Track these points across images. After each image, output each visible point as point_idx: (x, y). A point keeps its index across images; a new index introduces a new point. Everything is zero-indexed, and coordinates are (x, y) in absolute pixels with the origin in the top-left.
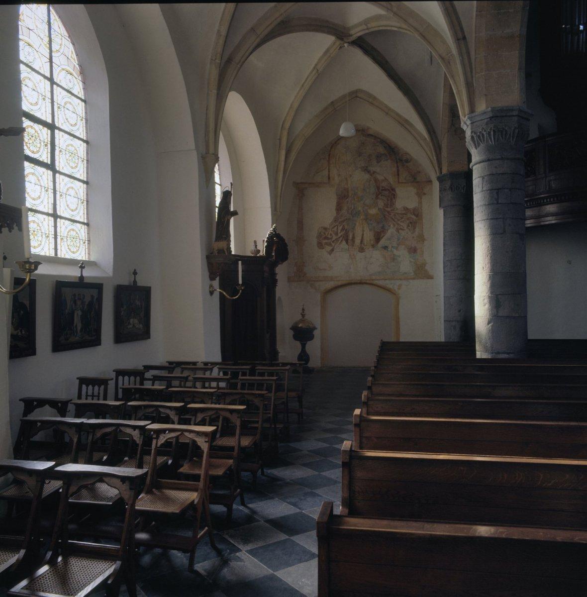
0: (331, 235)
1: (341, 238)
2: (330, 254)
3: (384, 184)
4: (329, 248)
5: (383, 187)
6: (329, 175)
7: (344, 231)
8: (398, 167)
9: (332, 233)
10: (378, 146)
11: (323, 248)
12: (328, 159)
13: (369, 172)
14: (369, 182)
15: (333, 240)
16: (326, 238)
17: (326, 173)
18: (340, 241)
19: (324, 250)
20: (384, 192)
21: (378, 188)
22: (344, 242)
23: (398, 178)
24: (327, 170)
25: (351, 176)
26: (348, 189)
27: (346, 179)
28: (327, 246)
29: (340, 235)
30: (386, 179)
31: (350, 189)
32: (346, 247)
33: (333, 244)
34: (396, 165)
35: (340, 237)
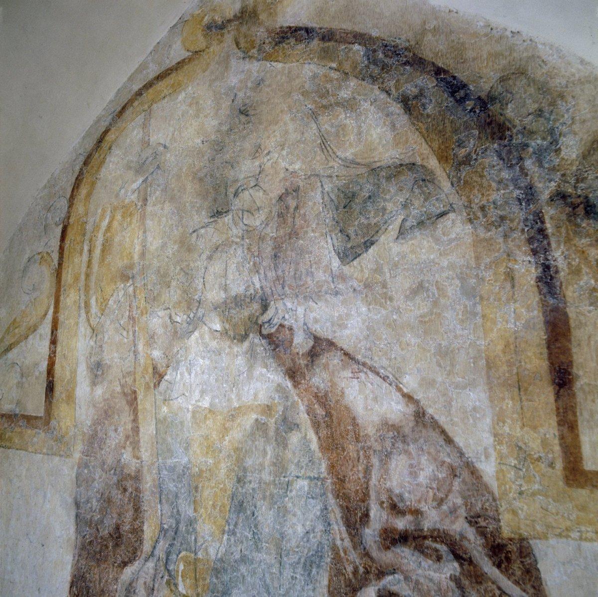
3: (409, 476)
5: (395, 508)
6: (50, 371)
8: (547, 279)
10: (350, 105)
12: (55, 256)
13: (276, 342)
14: (282, 443)
17: (39, 346)
20: (405, 555)
21: (355, 518)
23: (568, 422)
24: (46, 329)
25: (159, 376)
26: (137, 477)
27: (132, 400)
30: (420, 415)
31: (148, 483)
34: (526, 269)
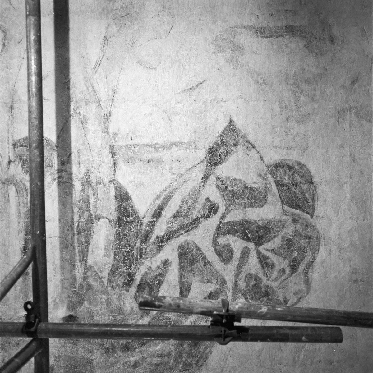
0: (225, 255)
1: (160, 230)
2: (231, 127)
4: (239, 168)
7: (138, 278)
9: (218, 265)
11: (277, 166)
15: (215, 220)
16: (257, 234)
18: (168, 213)
19: (273, 157)
22: (142, 205)
28: (252, 179)
29: (170, 252)
32: (127, 177)
33: (212, 192)
35: (169, 237)
